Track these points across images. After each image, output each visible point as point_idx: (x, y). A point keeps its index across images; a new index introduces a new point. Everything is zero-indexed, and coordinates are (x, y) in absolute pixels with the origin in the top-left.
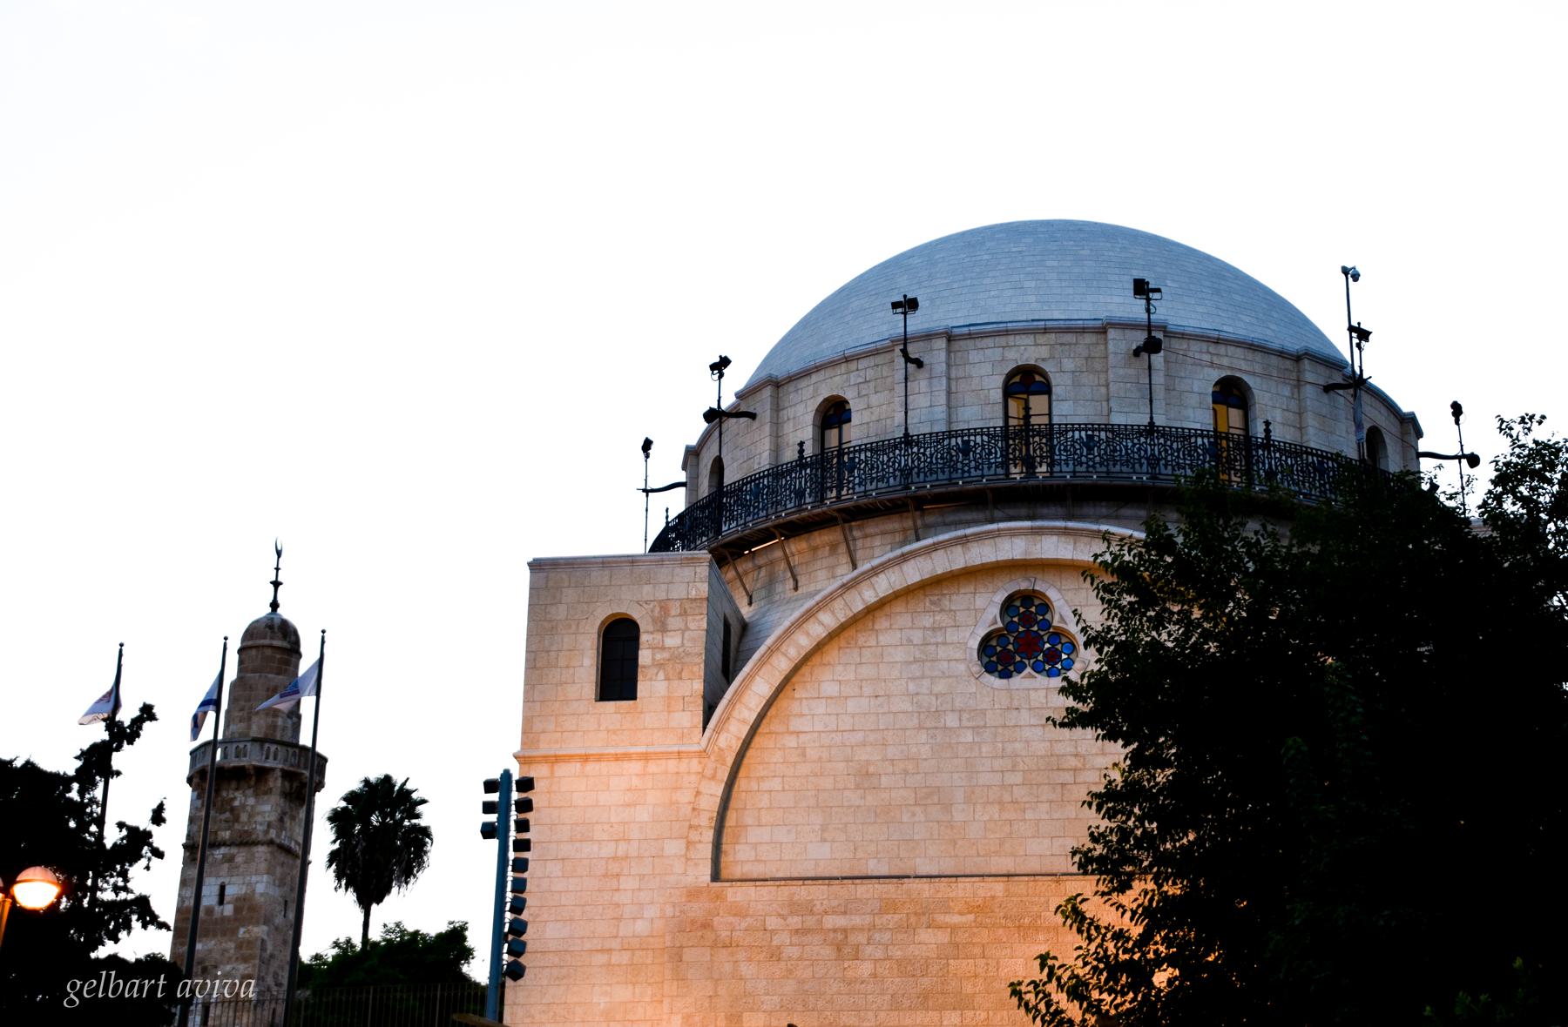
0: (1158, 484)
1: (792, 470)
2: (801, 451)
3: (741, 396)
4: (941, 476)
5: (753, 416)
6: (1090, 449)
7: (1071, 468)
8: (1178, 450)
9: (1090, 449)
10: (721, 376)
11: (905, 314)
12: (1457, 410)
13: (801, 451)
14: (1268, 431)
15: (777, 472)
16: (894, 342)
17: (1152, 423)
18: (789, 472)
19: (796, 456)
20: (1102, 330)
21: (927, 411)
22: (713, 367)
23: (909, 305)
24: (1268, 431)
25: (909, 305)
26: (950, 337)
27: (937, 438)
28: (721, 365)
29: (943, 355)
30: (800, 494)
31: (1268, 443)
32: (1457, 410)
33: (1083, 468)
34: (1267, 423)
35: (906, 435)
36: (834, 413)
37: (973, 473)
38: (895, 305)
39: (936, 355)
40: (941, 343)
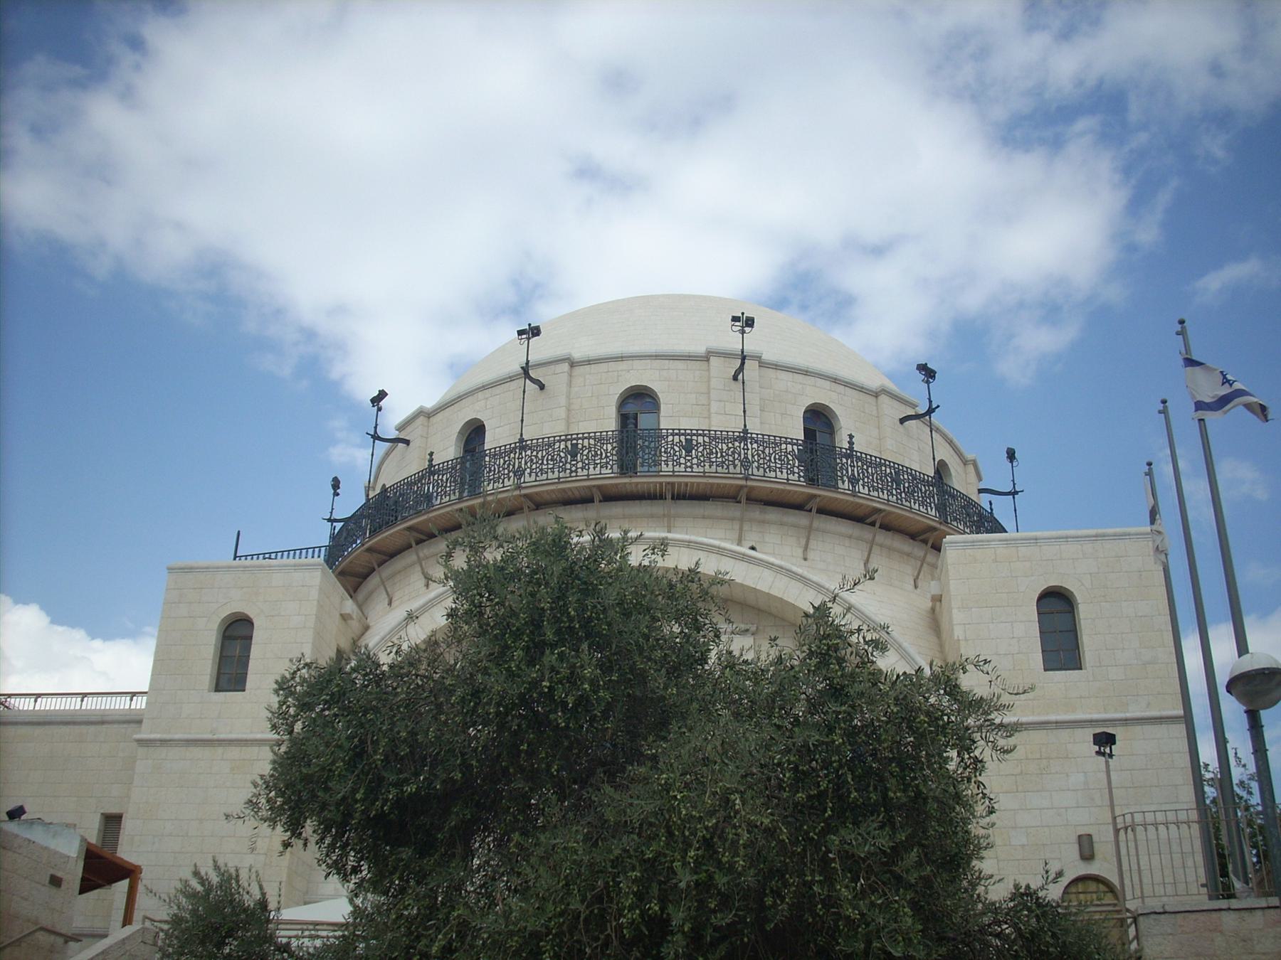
0: (749, 483)
2: (431, 460)
3: (401, 428)
5: (407, 442)
6: (689, 452)
8: (770, 455)
9: (689, 452)
11: (529, 339)
12: (1011, 455)
13: (431, 460)
14: (851, 443)
17: (745, 431)
20: (706, 357)
21: (546, 422)
23: (535, 331)
24: (851, 443)
25: (535, 331)
26: (573, 364)
29: (565, 377)
31: (850, 454)
32: (1011, 455)
34: (851, 436)
35: (522, 440)
36: (475, 432)
39: (555, 379)
40: (566, 366)
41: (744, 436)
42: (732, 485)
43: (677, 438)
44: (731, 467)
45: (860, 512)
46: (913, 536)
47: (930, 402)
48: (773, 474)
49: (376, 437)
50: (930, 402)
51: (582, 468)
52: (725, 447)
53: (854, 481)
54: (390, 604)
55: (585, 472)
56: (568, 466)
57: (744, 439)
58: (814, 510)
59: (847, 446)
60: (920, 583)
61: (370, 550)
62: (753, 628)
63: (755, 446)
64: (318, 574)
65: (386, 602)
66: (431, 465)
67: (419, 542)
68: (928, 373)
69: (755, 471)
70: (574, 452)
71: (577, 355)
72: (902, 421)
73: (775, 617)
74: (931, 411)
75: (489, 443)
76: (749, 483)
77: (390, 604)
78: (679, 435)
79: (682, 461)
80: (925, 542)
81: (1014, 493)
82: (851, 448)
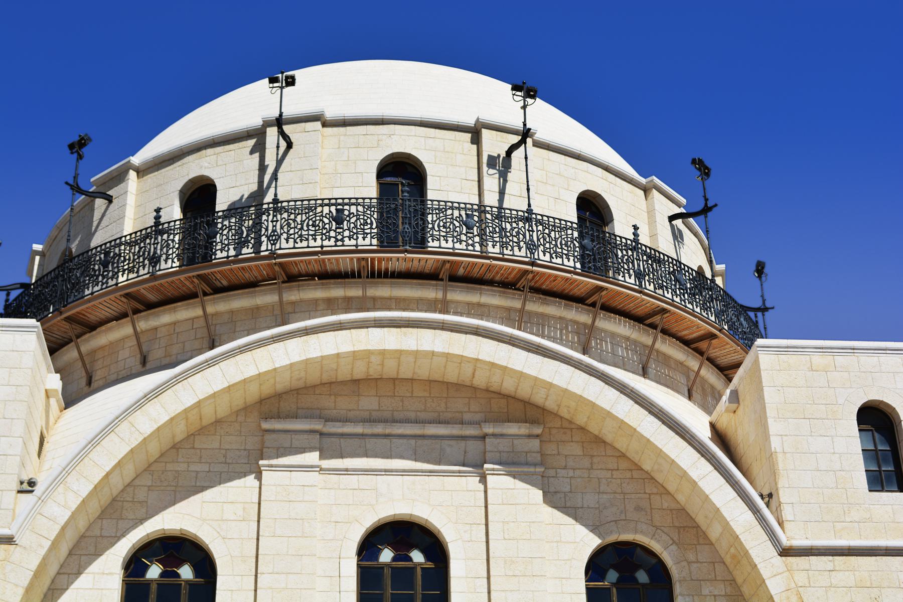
1: (147, 236)
2: (157, 218)
4: (312, 243)
7: (450, 245)
10: (80, 157)
11: (282, 88)
12: (760, 269)
13: (157, 218)
14: (635, 235)
16: (267, 124)
17: (530, 211)
18: (143, 239)
19: (151, 222)
22: (71, 147)
24: (635, 235)
25: (291, 82)
27: (309, 207)
28: (78, 146)
30: (155, 260)
31: (635, 244)
32: (760, 269)
33: (463, 246)
34: (636, 228)
37: (346, 239)
41: (528, 217)
42: (514, 268)
43: (456, 213)
44: (516, 249)
45: (640, 311)
46: (686, 342)
47: (706, 200)
48: (559, 261)
49: (77, 189)
50: (706, 200)
51: (350, 238)
52: (508, 227)
53: (639, 276)
54: (89, 383)
55: (353, 242)
56: (332, 234)
57: (528, 220)
58: (598, 305)
59: (632, 237)
60: (694, 394)
61: (68, 319)
62: (538, 430)
63: (540, 228)
64: (33, 337)
65: (83, 381)
66: (157, 222)
67: (136, 311)
68: (704, 170)
69: (541, 254)
70: (339, 219)
71: (330, 114)
72: (672, 218)
73: (561, 418)
74: (706, 210)
75: (221, 204)
76: (535, 268)
77: (89, 383)
78: (459, 209)
79: (463, 238)
80: (700, 353)
81: (764, 309)
82: (636, 240)
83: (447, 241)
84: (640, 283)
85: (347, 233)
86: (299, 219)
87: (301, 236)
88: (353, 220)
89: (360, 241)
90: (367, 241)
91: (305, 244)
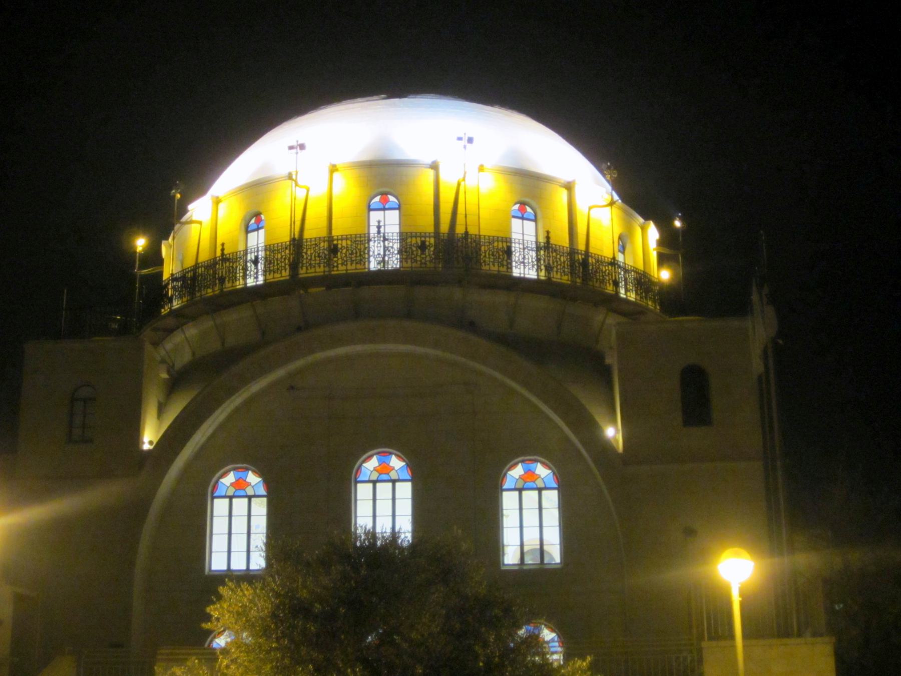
4: (318, 270)
14: (548, 238)
15: (212, 264)
17: (467, 233)
24: (548, 238)
37: (340, 267)
38: (291, 148)
51: (342, 264)
78: (416, 237)
79: (419, 259)
83: (407, 262)
84: (549, 273)
85: (340, 262)
86: (309, 253)
87: (310, 264)
88: (344, 251)
89: (349, 267)
90: (354, 265)
91: (313, 270)
